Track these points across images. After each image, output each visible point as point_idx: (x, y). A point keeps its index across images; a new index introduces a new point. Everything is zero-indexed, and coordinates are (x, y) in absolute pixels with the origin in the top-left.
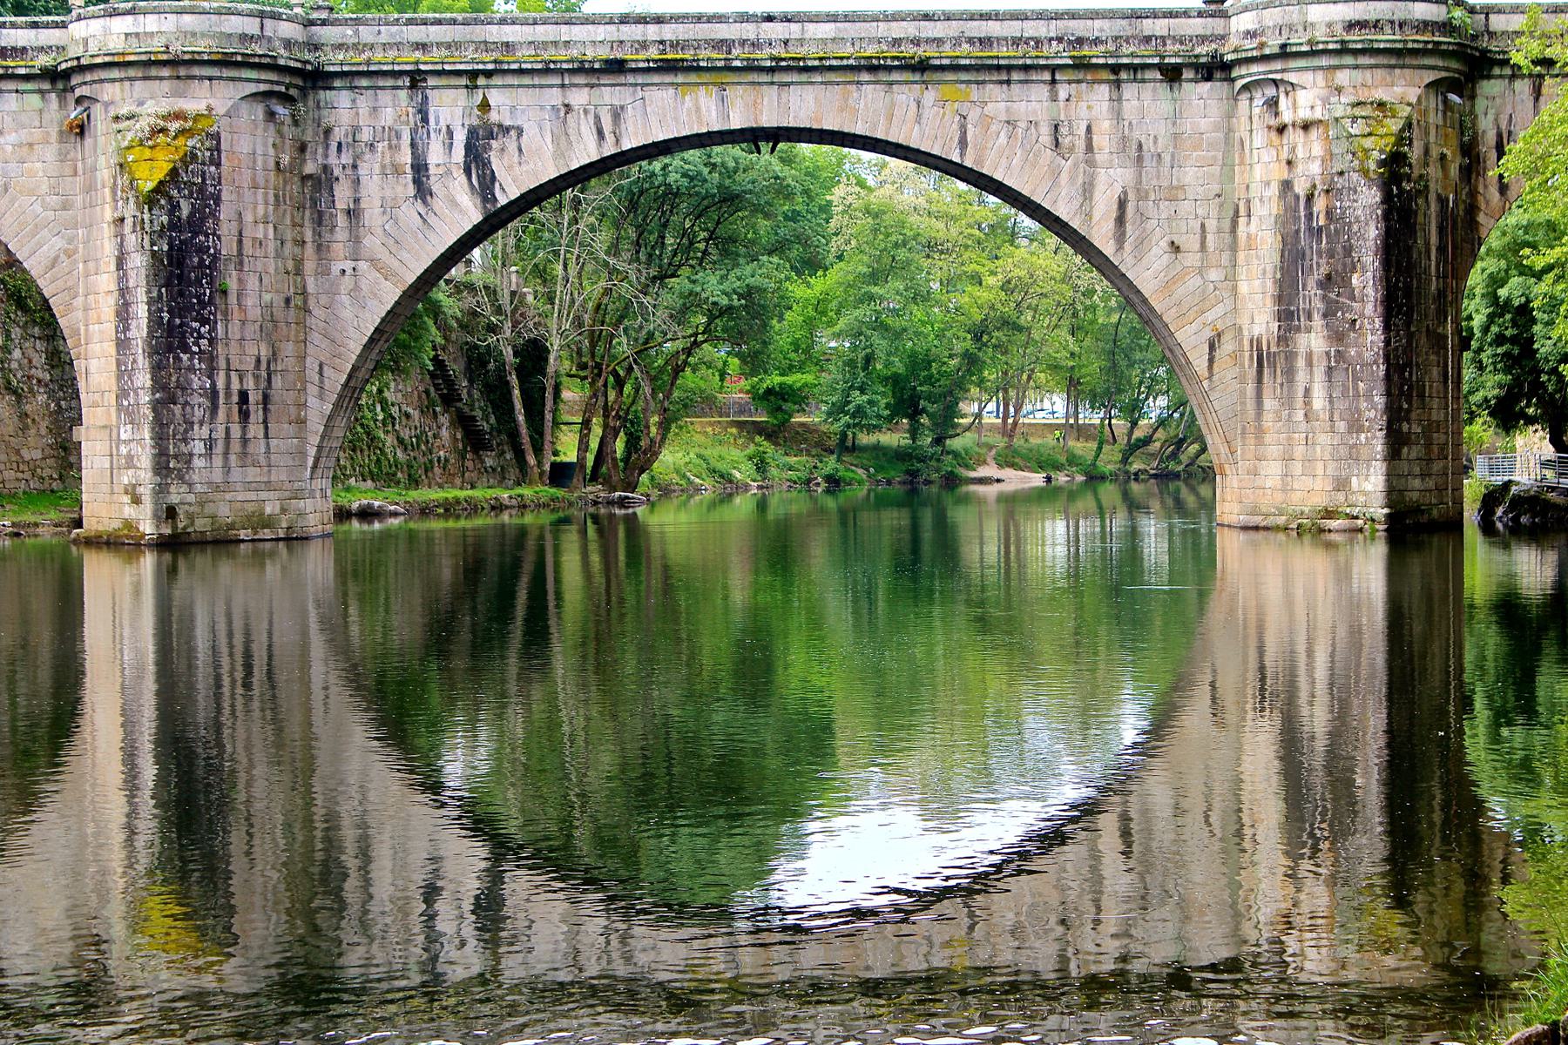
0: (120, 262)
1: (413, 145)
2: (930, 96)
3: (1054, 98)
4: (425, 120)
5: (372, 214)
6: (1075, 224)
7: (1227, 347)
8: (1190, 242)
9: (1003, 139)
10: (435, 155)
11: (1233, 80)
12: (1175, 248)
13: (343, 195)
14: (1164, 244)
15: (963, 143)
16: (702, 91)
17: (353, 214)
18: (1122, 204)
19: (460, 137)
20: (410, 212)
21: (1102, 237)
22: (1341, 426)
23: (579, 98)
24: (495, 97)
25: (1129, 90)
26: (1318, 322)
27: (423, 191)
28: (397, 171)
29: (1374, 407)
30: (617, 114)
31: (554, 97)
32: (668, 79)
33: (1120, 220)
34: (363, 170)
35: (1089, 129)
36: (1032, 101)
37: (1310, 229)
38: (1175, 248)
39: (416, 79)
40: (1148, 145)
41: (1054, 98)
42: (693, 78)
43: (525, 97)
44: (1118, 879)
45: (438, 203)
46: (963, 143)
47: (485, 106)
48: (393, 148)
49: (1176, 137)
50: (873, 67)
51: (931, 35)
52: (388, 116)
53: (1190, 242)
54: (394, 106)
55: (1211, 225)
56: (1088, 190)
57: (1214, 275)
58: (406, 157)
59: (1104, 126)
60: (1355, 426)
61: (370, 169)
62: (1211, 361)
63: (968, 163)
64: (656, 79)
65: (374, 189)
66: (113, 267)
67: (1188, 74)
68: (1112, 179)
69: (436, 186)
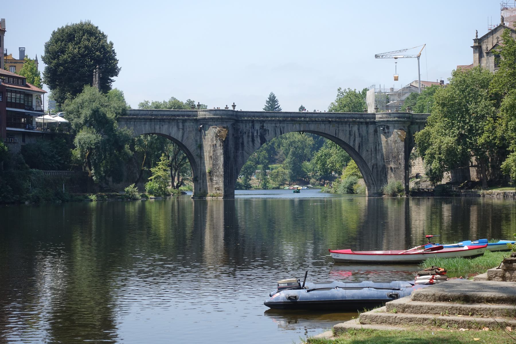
4: (254, 128)
8: (370, 150)
9: (342, 133)
10: (255, 134)
11: (376, 125)
12: (367, 151)
13: (241, 140)
16: (297, 124)
18: (359, 144)
21: (357, 149)
23: (278, 125)
24: (265, 125)
25: (361, 126)
30: (283, 128)
31: (273, 125)
32: (292, 122)
33: (359, 147)
34: (244, 136)
35: (355, 131)
38: (367, 151)
39: (253, 121)
41: (349, 127)
42: (295, 122)
43: (269, 125)
46: (336, 134)
50: (323, 121)
51: (331, 116)
59: (357, 131)
61: (245, 137)
62: (373, 169)
63: (337, 137)
64: (290, 122)
67: (370, 123)
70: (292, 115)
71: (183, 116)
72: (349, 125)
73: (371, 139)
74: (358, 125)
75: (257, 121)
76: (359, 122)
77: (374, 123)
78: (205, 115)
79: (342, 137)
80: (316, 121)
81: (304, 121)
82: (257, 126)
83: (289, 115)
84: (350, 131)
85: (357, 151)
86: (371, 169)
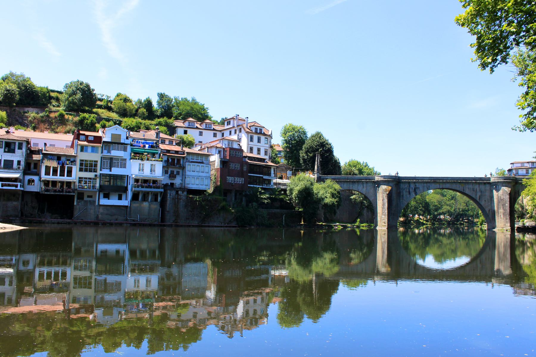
0: (383, 200)
1: (409, 189)
2: (460, 185)
3: (473, 185)
5: (404, 196)
6: (475, 198)
7: (490, 211)
9: (468, 190)
10: (411, 190)
12: (485, 201)
13: (401, 194)
14: (484, 200)
15: (464, 190)
17: (403, 196)
18: (480, 196)
19: (413, 188)
20: (408, 196)
21: (478, 199)
22: (505, 219)
23: (425, 185)
24: (417, 185)
25: (480, 185)
26: (502, 209)
27: (410, 193)
28: (407, 191)
29: (508, 217)
31: (423, 185)
33: (480, 198)
36: (471, 186)
37: (501, 199)
38: (485, 201)
39: (409, 183)
40: (482, 191)
44: (479, 266)
45: (411, 195)
46: (464, 190)
47: (416, 185)
48: (407, 189)
49: (485, 190)
52: (406, 186)
53: (487, 200)
54: (407, 186)
55: (489, 199)
56: (476, 195)
57: (489, 204)
58: (408, 190)
60: (506, 219)
65: (404, 193)
66: (382, 200)
68: (479, 194)
69: (411, 193)
70: (434, 178)
71: (366, 179)
72: (473, 184)
73: (487, 194)
74: (479, 184)
75: (412, 182)
76: (479, 183)
77: (490, 183)
78: (378, 179)
79: (467, 191)
80: (450, 182)
81: (442, 182)
82: (412, 186)
83: (432, 178)
84: (473, 189)
85: (478, 201)
86: (488, 212)
